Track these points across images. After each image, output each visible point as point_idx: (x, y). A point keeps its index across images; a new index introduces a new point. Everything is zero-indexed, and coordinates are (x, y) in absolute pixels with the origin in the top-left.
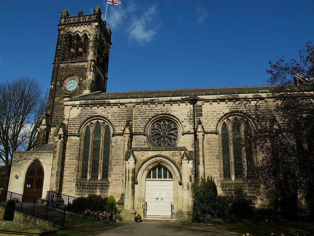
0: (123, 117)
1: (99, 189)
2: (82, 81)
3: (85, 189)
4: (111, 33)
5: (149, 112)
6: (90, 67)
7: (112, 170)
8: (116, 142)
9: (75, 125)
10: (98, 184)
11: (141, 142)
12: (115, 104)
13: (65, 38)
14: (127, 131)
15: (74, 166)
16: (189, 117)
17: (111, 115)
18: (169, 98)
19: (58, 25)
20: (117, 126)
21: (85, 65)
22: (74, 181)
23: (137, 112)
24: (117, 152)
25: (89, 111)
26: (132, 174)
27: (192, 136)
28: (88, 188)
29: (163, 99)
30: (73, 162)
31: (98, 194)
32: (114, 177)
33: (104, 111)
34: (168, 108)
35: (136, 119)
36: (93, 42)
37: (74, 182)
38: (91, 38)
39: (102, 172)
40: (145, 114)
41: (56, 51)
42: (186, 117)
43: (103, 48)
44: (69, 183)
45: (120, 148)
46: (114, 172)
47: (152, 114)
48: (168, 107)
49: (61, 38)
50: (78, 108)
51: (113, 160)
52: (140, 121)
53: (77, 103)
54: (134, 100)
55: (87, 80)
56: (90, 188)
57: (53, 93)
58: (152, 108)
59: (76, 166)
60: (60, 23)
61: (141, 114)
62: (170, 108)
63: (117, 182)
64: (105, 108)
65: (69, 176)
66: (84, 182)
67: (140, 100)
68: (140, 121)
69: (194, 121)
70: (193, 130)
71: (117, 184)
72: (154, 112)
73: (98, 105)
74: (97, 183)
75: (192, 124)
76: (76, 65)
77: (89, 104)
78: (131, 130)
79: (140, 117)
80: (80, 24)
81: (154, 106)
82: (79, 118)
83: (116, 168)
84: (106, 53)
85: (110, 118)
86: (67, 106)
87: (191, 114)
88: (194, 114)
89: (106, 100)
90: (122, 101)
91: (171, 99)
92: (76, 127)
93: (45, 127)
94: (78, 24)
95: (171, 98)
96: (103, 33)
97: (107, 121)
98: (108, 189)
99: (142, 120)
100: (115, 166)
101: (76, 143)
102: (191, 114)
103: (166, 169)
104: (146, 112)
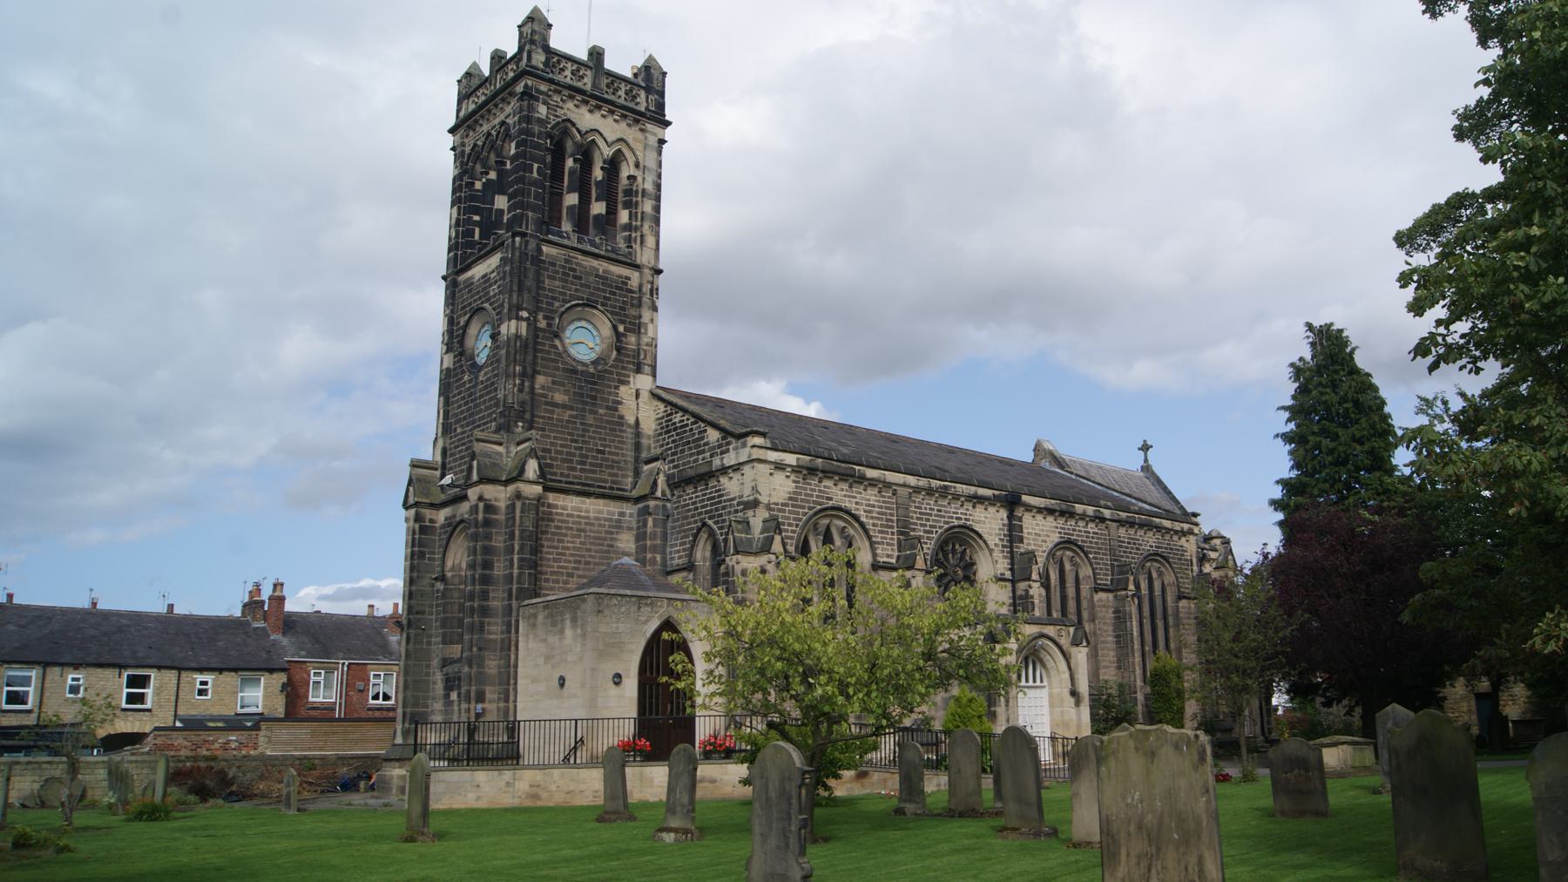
0: (887, 520)
2: (625, 336)
5: (936, 515)
12: (873, 483)
17: (865, 511)
18: (972, 490)
21: (629, 279)
23: (915, 512)
25: (814, 490)
33: (849, 496)
35: (914, 530)
36: (654, 202)
40: (928, 520)
48: (967, 510)
53: (791, 459)
54: (912, 480)
57: (530, 358)
61: (921, 519)
64: (851, 487)
67: (923, 482)
73: (837, 478)
76: (601, 266)
79: (922, 525)
80: (606, 107)
82: (793, 506)
85: (863, 519)
87: (1004, 535)
88: (1010, 535)
89: (857, 468)
90: (891, 477)
94: (595, 100)
102: (1004, 535)
104: (931, 515)
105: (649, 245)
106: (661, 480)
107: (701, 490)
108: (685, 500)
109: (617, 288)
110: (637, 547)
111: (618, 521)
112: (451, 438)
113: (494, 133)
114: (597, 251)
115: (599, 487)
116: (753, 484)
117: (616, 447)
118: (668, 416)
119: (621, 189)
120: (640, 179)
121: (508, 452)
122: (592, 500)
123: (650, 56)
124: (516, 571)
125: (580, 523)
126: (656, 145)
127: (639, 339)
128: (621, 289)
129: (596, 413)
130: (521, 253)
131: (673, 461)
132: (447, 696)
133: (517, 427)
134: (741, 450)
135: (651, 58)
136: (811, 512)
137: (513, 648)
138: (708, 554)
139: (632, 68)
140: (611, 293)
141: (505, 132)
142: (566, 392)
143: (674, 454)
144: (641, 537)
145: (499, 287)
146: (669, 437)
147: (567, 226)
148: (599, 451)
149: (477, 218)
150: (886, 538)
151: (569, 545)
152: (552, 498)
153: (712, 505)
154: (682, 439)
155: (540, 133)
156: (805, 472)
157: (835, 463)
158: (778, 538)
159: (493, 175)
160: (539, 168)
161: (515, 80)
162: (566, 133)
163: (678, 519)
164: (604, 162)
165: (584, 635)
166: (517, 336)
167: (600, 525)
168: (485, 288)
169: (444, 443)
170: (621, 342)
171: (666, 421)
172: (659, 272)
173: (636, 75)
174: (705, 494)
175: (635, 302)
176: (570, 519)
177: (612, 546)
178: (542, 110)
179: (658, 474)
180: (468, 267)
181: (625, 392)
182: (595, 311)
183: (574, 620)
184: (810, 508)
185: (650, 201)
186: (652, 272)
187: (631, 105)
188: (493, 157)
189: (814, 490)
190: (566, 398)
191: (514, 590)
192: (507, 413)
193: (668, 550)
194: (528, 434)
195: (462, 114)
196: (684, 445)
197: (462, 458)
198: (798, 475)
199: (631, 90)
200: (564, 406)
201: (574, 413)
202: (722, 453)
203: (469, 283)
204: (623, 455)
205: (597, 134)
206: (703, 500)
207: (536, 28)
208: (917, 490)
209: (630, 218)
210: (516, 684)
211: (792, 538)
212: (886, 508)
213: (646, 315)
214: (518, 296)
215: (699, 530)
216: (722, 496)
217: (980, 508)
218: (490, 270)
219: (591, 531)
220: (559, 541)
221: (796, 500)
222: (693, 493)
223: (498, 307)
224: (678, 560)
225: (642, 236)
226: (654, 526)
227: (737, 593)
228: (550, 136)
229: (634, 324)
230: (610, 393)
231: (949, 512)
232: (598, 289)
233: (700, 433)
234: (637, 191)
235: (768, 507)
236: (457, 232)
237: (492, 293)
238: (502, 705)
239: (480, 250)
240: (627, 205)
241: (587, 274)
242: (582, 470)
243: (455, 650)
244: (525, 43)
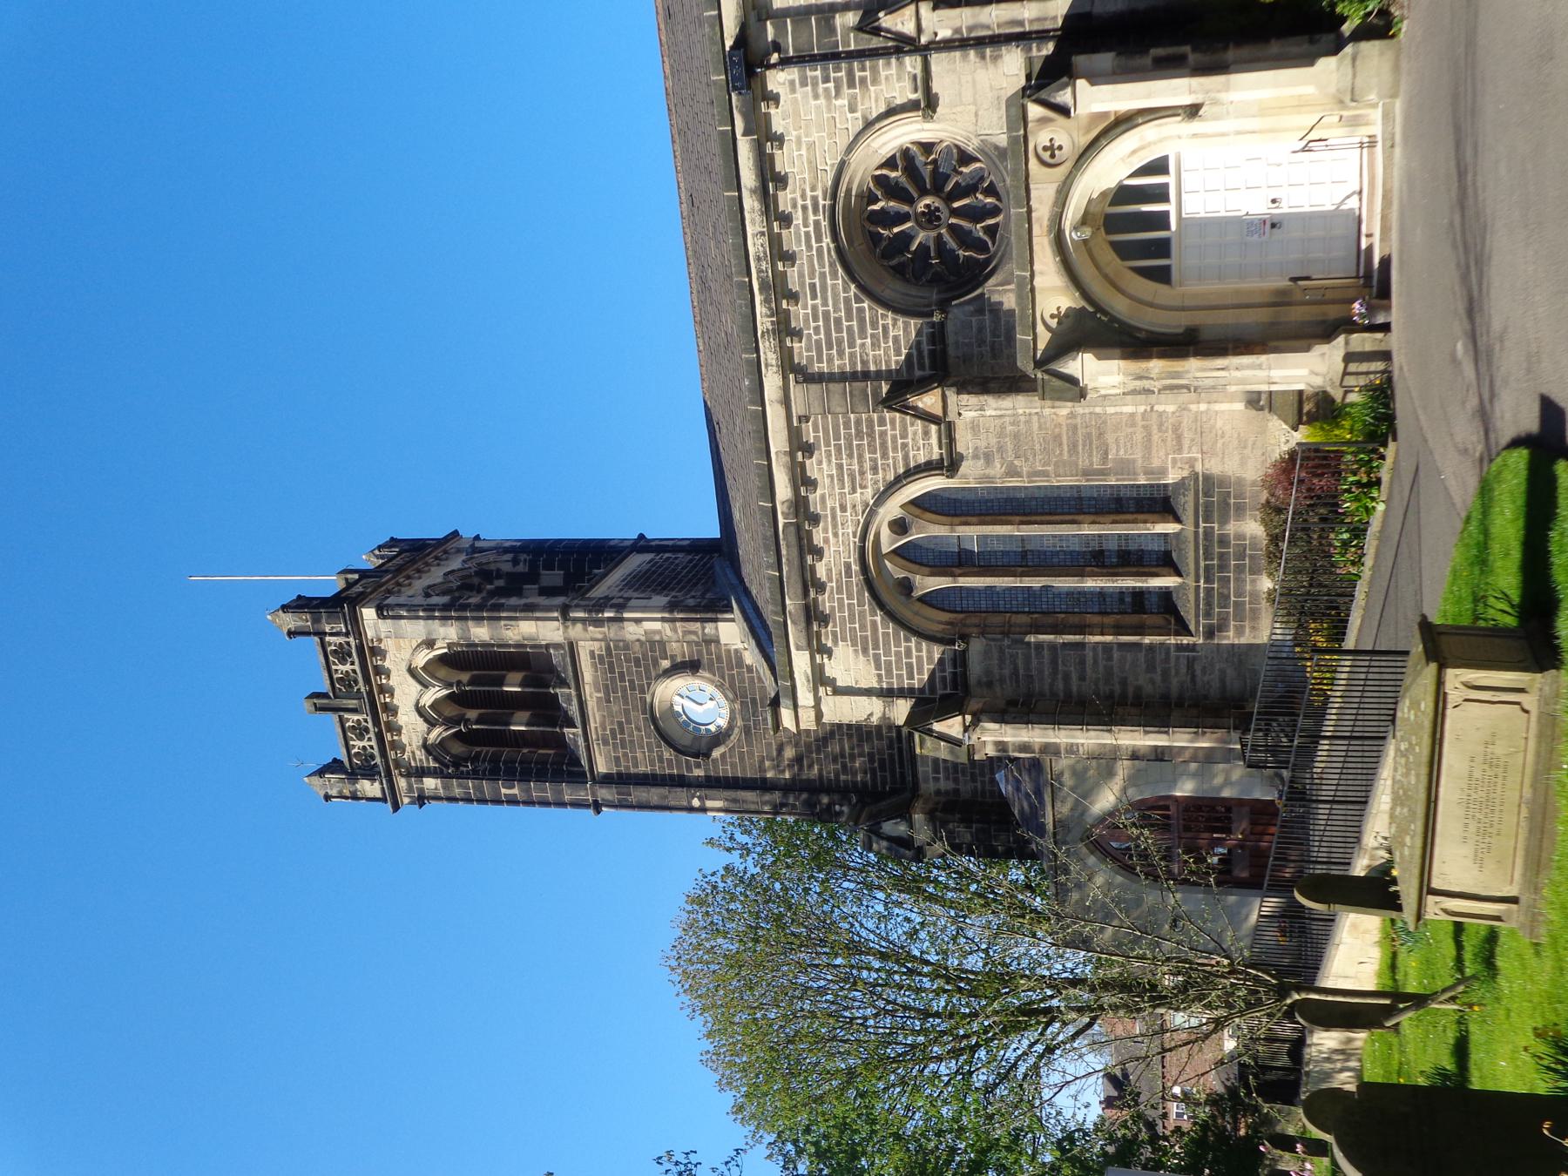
0: (859, 435)
1: (1224, 521)
2: (673, 657)
3: (1226, 591)
4: (393, 542)
5: (825, 304)
6: (598, 623)
7: (1125, 467)
8: (988, 458)
9: (909, 666)
10: (1201, 530)
11: (981, 330)
12: (802, 480)
13: (456, 765)
14: (929, 401)
16: (838, 89)
17: (854, 491)
18: (751, 204)
19: (396, 807)
20: (906, 457)
21: (592, 653)
23: (830, 360)
24: (1037, 447)
25: (841, 601)
26: (1149, 357)
27: (938, 62)
28: (1220, 579)
29: (754, 235)
30: (1095, 662)
31: (1252, 528)
32: (1162, 453)
33: (835, 526)
34: (800, 202)
35: (864, 363)
38: (448, 634)
39: (1141, 517)
40: (838, 321)
41: (529, 803)
42: (843, 102)
43: (486, 574)
44: (1198, 672)
45: (1016, 436)
46: (1138, 455)
47: (834, 286)
48: (794, 206)
49: (460, 786)
51: (1077, 465)
52: (873, 344)
53: (801, 662)
55: (666, 628)
56: (1223, 567)
57: (749, 796)
58: (802, 284)
60: (384, 800)
61: (840, 342)
62: (798, 194)
63: (1187, 436)
65: (1166, 674)
66: (1192, 597)
67: (769, 353)
68: (875, 345)
69: (861, 55)
70: (908, 60)
71: (1198, 439)
72: (823, 275)
73: (809, 559)
74: (1196, 533)
75: (875, 70)
78: (922, 386)
79: (852, 345)
81: (793, 277)
82: (876, 647)
83: (1118, 446)
84: (509, 557)
85: (869, 495)
86: (819, 715)
87: (826, 80)
89: (781, 521)
91: (753, 191)
92: (919, 659)
93: (918, 817)
94: (380, 709)
95: (745, 194)
96: (409, 577)
97: (881, 511)
98: (1223, 482)
99: (870, 331)
100: (1106, 453)
101: (1001, 651)
103: (1124, 194)
104: (826, 315)
105: (534, 630)
109: (612, 671)
126: (389, 621)
128: (611, 664)
140: (622, 679)
150: (894, 438)
157: (785, 569)
182: (656, 702)
184: (873, 614)
186: (569, 623)
208: (789, 366)
212: (837, 438)
217: (785, 161)
231: (810, 258)
232: (625, 697)
241: (611, 715)
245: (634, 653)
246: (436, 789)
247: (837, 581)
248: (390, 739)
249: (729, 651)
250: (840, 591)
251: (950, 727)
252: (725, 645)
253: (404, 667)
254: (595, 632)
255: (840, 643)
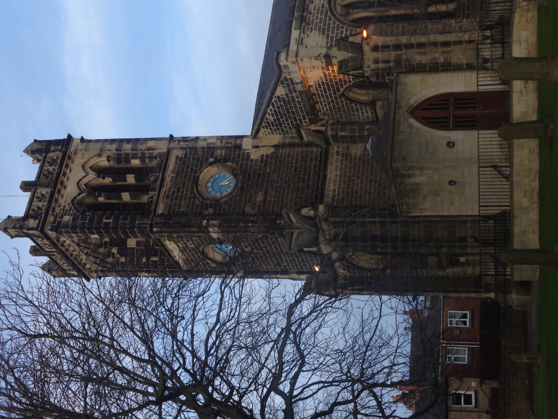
2: (216, 157)
15: (430, 27)
22: (459, 22)
25: (317, 17)
36: (124, 143)
37: (462, 22)
50: (306, 35)
53: (295, 34)
59: (429, 24)
76: (169, 175)
77: (302, 16)
82: (328, 31)
106: (313, 127)
107: (320, 98)
108: (327, 110)
109: (184, 164)
110: (361, 142)
111: (342, 155)
112: (290, 269)
113: (86, 251)
114: (160, 178)
115: (320, 169)
116: (313, 59)
117: (292, 159)
118: (269, 125)
119: (116, 166)
120: (109, 153)
121: (298, 228)
122: (328, 173)
123: (24, 151)
124: (377, 219)
125: (344, 181)
126: (85, 144)
127: (217, 148)
128: (185, 162)
129: (269, 173)
130: (164, 227)
131: (300, 120)
132: (463, 264)
133: (280, 223)
134: (290, 70)
135: (26, 151)
136: (333, 19)
137: (430, 219)
138: (364, 92)
139: (34, 163)
140: (188, 168)
141: (84, 243)
142: (256, 193)
143: (295, 118)
144: (353, 140)
145: (188, 241)
146: (284, 124)
147: (145, 199)
148: (295, 170)
149: (144, 260)
151: (359, 186)
152: (328, 199)
153: (329, 90)
154: (285, 114)
155: (81, 219)
156: (304, 24)
158: (351, 39)
159: (114, 250)
160: (106, 219)
161: (48, 237)
162: (81, 203)
163: (341, 115)
164: (99, 177)
165: (421, 168)
166: (220, 226)
167: (346, 167)
168: (190, 250)
169: (294, 273)
170: (220, 159)
171: (273, 126)
172: (171, 136)
173: (38, 161)
174: (322, 95)
175: (193, 152)
176: (342, 186)
177: (360, 159)
178: (66, 218)
179: (309, 130)
180: (177, 263)
181: (255, 155)
182: (201, 177)
183: (410, 176)
184: (330, 19)
185: (124, 146)
186: (172, 141)
187: (59, 161)
188: (102, 250)
189: (317, 17)
190: (260, 193)
191: (390, 220)
192: (271, 230)
193: (362, 121)
194: (285, 216)
195: (75, 273)
196: (288, 112)
197: (303, 260)
198: (306, 28)
199: (49, 163)
200: (266, 194)
201: (270, 187)
202: (293, 83)
203: (186, 262)
204: (298, 154)
205: (81, 182)
206: (327, 96)
207: (11, 226)
209: (136, 158)
210: (454, 216)
211: (351, 31)
213: (201, 144)
214: (192, 227)
215: (347, 98)
216: (323, 82)
218: (177, 247)
219: (349, 173)
220: (357, 193)
221: (324, 29)
222: (322, 104)
223: (201, 240)
224: (368, 114)
225: (148, 149)
226: (345, 130)
227: (390, 66)
228: (83, 213)
229: (208, 152)
230: (256, 165)
233: (280, 101)
234: (117, 154)
235: (329, 48)
236: (154, 272)
237: (193, 246)
238: (468, 225)
239: (164, 255)
240: (128, 161)
242: (309, 181)
243: (432, 260)
244: (22, 232)
245: (198, 156)
246: (69, 221)
247: (317, 10)
248: (57, 197)
249: (244, 153)
250: (318, 13)
251: (357, 39)
252: (245, 150)
253: (81, 165)
254: (183, 144)
255: (313, 31)
